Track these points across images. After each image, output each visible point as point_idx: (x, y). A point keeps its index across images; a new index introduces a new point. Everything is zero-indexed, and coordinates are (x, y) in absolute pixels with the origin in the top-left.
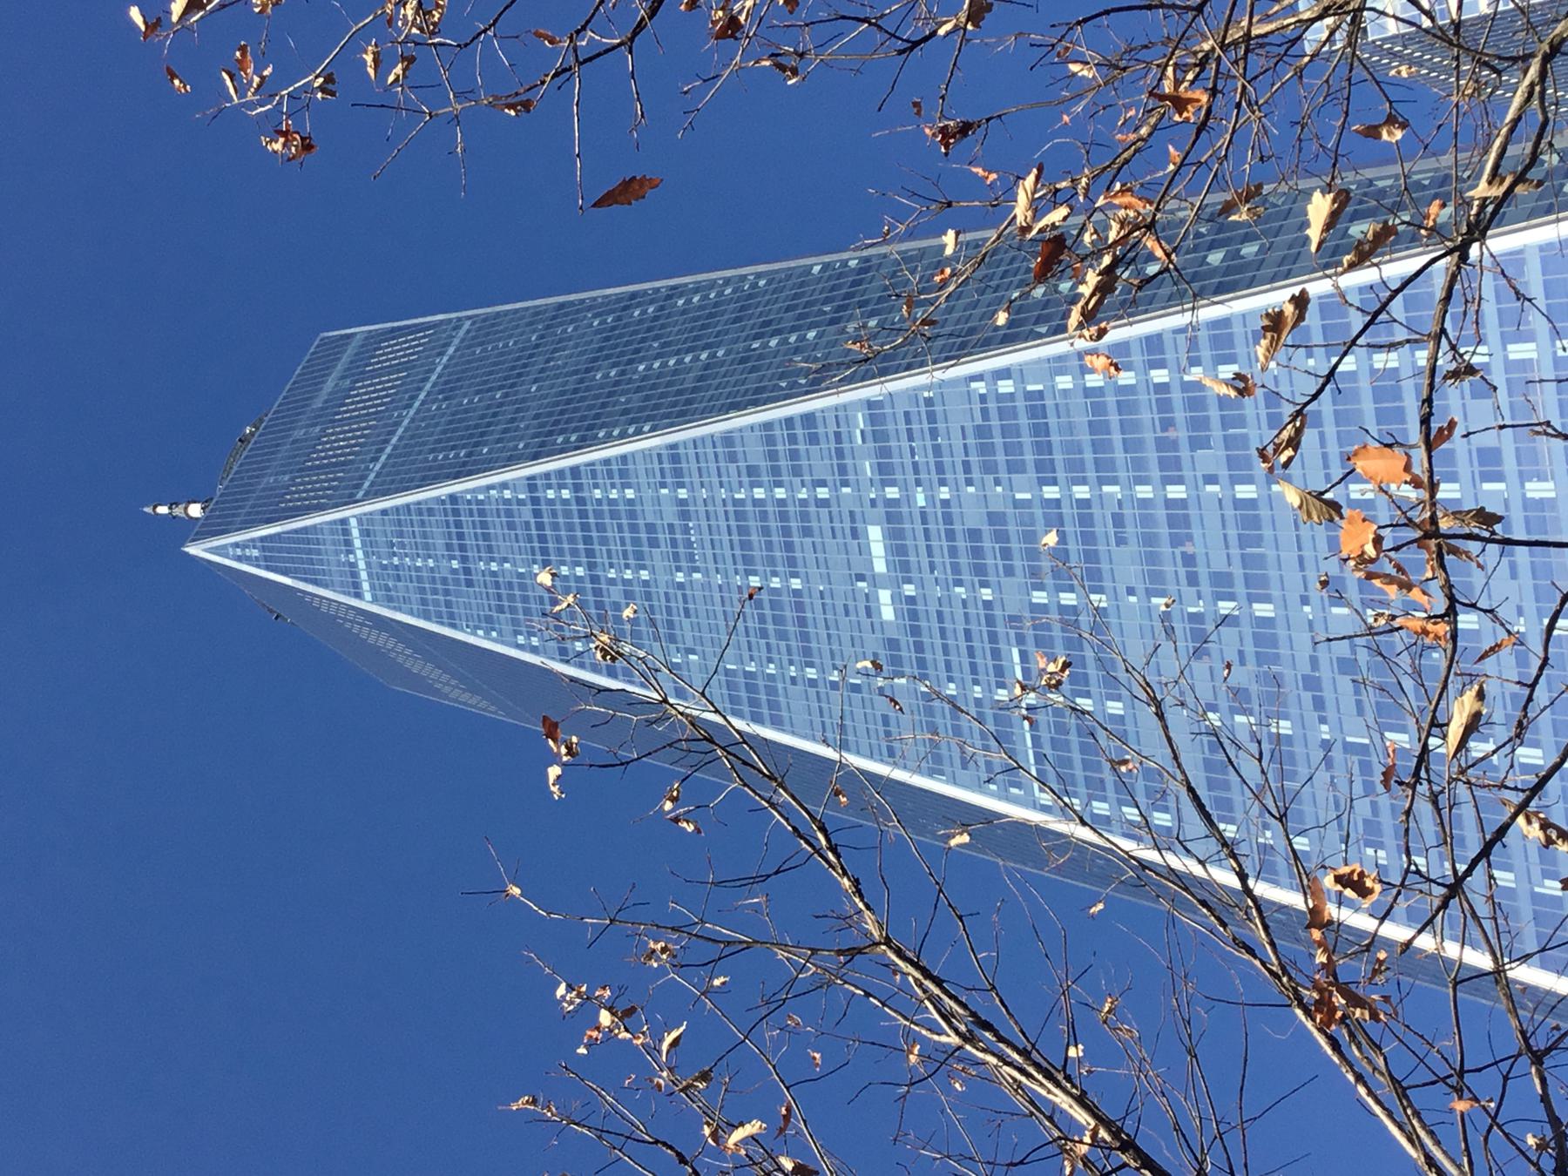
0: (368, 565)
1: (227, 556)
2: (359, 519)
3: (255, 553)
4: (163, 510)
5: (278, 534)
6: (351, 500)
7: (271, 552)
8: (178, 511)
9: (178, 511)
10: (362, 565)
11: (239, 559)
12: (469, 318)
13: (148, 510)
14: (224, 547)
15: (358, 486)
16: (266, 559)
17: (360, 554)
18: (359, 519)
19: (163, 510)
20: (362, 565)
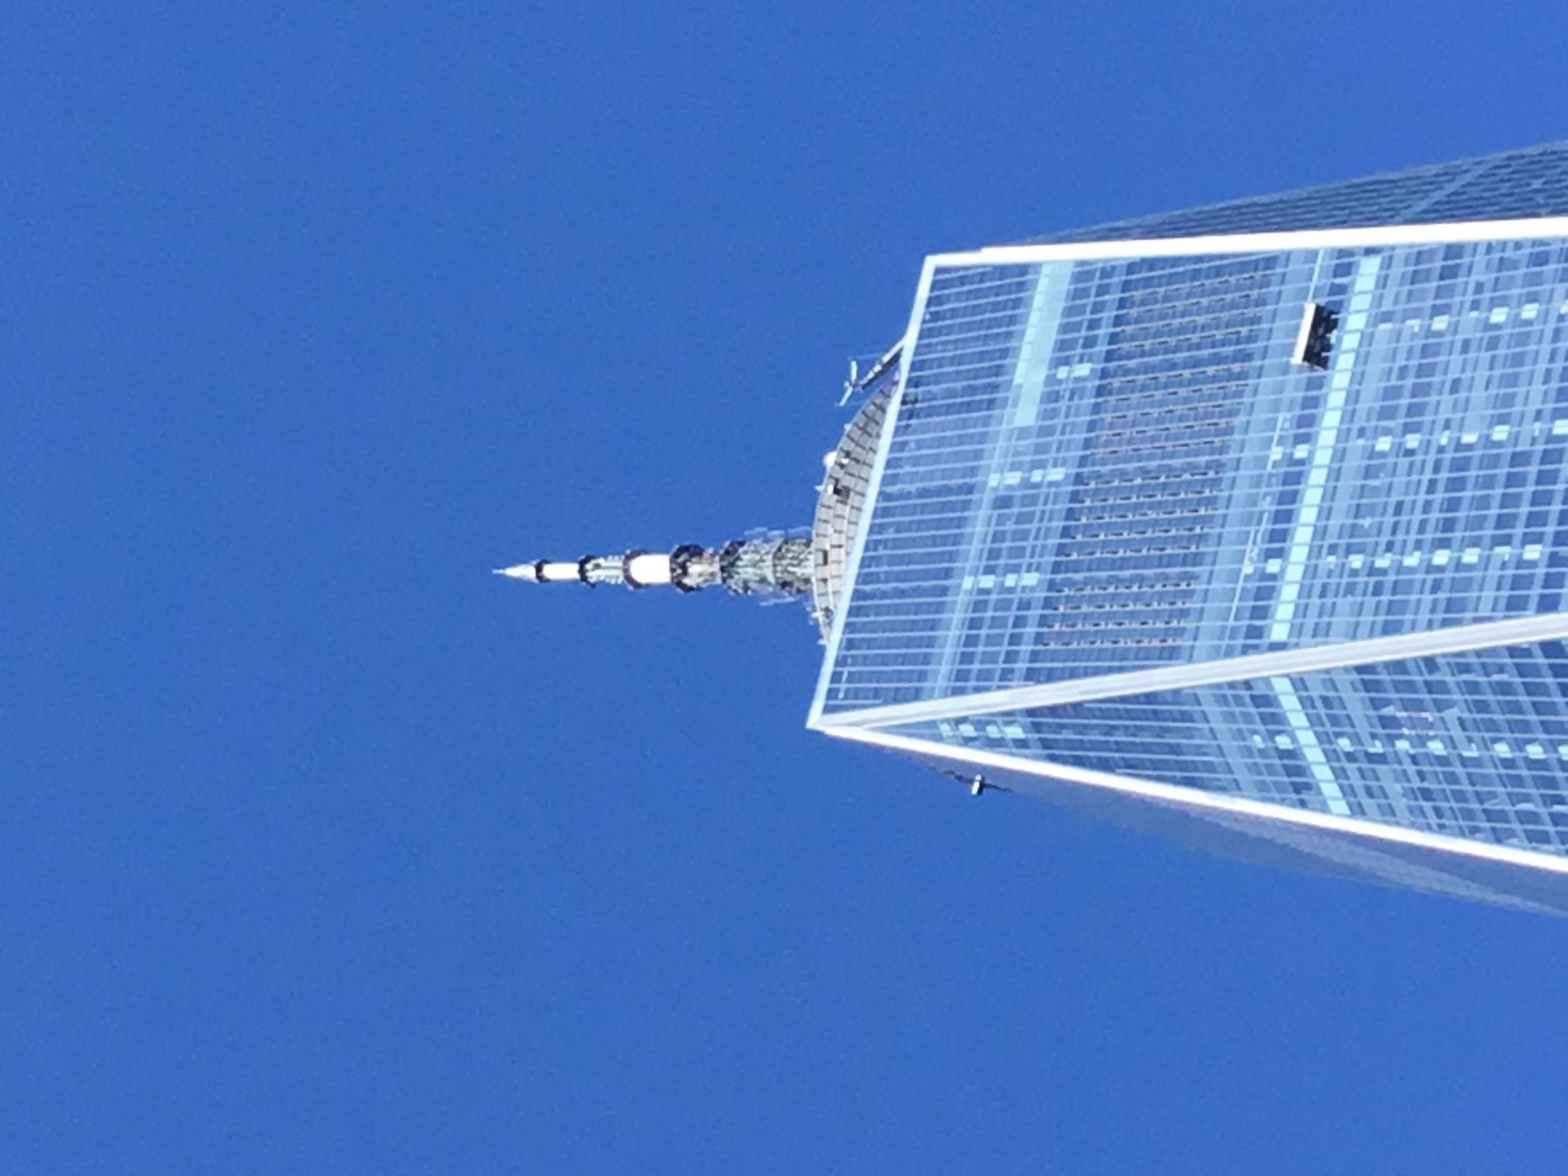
0: (1331, 756)
1: (938, 738)
2: (1299, 683)
3: (1015, 732)
4: (562, 571)
5: (1077, 708)
6: (1254, 639)
7: (1049, 730)
8: (606, 570)
9: (606, 570)
10: (1313, 754)
11: (967, 741)
12: (1370, 251)
13: (526, 572)
14: (932, 724)
15: (1261, 613)
16: (1046, 744)
17: (1307, 738)
18: (1299, 683)
19: (562, 571)
20: (1313, 754)
